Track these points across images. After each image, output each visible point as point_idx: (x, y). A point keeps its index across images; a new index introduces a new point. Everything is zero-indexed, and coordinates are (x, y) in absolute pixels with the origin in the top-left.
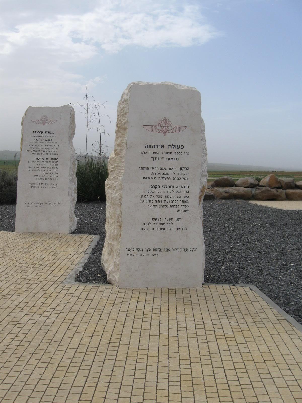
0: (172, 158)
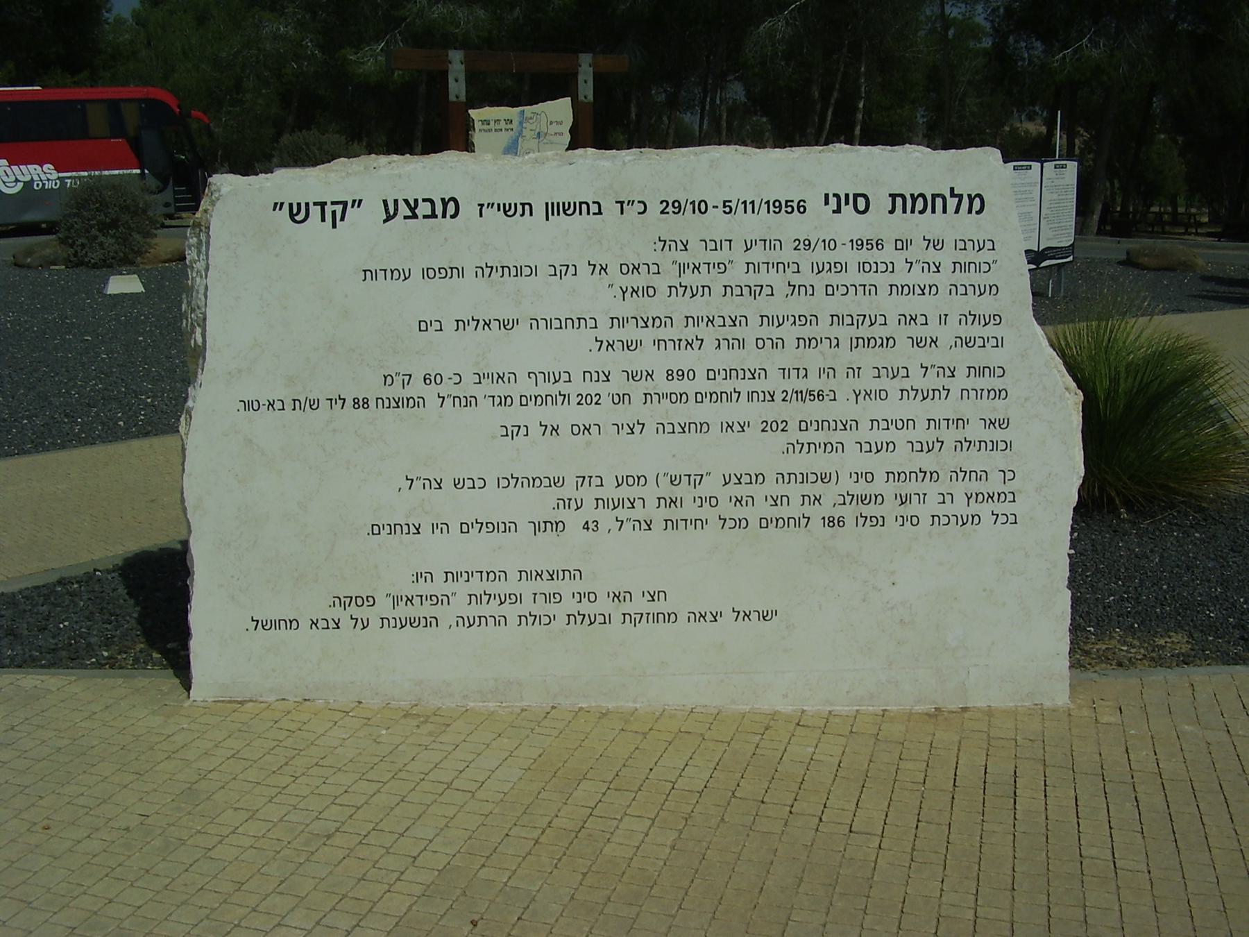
0: (416, 201)
